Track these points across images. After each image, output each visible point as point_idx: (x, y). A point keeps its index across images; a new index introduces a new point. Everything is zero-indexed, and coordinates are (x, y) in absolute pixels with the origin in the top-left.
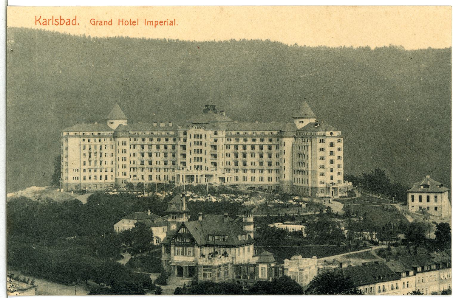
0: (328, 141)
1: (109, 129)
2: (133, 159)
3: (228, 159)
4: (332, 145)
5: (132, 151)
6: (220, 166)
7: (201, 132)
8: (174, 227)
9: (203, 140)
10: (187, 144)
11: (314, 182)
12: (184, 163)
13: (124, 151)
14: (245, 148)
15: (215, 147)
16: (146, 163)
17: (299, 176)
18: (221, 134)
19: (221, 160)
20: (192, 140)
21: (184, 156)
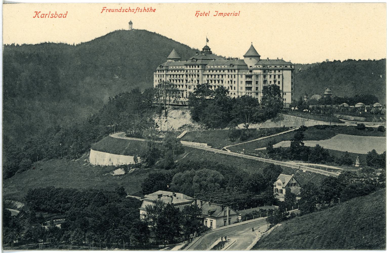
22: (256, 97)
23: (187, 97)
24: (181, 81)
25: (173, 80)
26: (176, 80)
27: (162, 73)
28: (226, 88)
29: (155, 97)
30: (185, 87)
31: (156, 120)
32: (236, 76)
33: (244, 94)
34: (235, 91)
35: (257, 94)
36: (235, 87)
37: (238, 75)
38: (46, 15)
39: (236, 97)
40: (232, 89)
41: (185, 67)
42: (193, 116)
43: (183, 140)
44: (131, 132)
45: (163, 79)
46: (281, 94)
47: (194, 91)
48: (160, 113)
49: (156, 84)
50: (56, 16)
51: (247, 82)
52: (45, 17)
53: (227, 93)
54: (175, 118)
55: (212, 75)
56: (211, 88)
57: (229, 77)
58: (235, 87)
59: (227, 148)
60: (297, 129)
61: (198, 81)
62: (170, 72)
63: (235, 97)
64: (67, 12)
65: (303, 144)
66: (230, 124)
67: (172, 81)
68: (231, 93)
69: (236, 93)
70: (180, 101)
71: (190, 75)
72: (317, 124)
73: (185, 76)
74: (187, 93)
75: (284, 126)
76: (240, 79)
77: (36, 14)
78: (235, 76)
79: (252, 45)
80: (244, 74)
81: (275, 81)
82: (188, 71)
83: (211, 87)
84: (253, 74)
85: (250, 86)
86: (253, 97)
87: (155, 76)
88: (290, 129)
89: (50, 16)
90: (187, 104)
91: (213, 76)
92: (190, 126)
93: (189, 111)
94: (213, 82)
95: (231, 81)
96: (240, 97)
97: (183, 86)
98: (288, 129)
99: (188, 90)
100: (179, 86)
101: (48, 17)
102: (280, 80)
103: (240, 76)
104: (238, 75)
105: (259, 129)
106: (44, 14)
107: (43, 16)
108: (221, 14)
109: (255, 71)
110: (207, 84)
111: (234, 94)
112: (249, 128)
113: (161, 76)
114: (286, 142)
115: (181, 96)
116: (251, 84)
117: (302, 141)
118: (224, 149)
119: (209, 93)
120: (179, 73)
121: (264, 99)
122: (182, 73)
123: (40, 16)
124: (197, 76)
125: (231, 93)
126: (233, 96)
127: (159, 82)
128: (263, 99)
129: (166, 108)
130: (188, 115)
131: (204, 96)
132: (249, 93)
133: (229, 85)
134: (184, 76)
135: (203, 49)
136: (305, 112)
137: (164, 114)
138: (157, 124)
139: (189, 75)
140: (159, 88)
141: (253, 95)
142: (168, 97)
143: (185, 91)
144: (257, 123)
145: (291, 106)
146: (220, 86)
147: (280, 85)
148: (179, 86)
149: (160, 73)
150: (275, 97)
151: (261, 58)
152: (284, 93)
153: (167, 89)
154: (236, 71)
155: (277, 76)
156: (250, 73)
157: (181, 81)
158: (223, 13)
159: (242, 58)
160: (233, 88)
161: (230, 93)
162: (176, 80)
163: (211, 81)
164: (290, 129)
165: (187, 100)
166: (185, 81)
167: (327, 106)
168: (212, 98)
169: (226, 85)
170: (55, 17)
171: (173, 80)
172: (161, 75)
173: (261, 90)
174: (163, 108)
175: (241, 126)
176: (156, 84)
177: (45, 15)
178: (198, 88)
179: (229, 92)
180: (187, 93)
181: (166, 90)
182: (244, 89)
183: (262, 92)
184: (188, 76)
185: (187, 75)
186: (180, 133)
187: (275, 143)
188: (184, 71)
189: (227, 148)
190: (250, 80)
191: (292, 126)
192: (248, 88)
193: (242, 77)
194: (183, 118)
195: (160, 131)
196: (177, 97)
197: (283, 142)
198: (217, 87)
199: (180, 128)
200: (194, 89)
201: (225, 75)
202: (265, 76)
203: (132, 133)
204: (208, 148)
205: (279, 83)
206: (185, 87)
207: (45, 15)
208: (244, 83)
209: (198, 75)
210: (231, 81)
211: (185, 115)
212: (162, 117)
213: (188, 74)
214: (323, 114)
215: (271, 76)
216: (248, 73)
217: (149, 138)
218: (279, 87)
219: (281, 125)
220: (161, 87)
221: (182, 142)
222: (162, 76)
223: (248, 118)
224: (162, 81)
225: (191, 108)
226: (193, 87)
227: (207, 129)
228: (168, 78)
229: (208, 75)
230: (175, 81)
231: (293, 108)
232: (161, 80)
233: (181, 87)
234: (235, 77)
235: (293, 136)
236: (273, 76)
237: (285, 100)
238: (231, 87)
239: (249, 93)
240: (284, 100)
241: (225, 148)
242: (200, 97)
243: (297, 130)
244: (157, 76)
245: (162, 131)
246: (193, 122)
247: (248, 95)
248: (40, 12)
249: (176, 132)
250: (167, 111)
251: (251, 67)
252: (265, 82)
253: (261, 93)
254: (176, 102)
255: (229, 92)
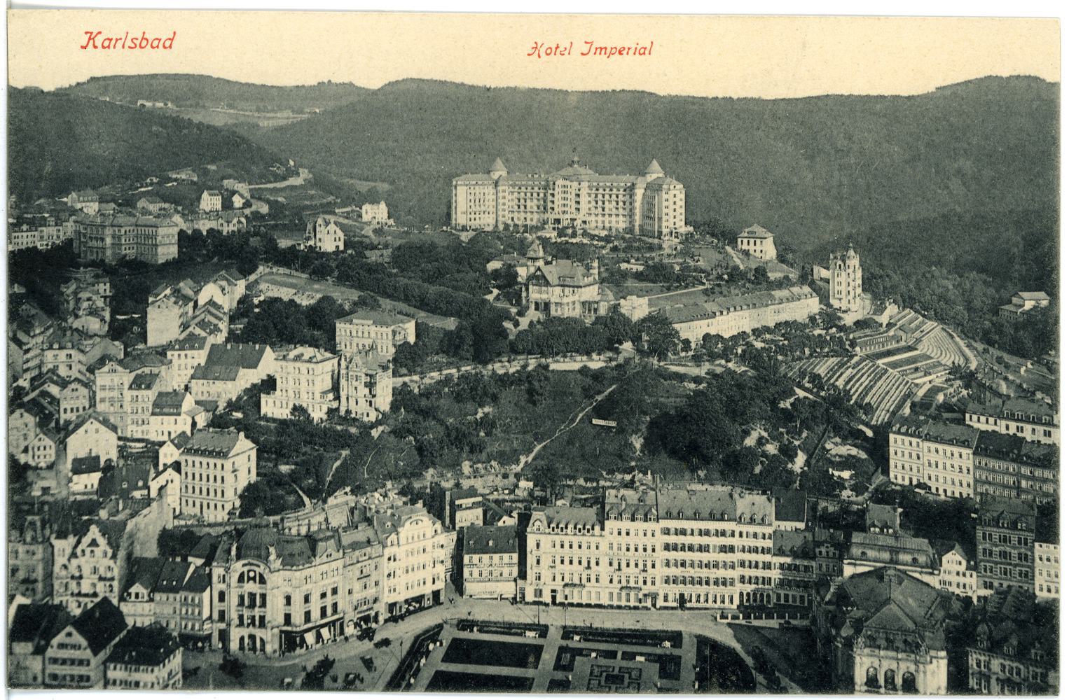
0: (672, 193)
1: (491, 179)
2: (510, 204)
3: (590, 206)
4: (675, 196)
5: (510, 197)
6: (583, 212)
7: (567, 183)
8: (532, 270)
9: (569, 189)
10: (556, 193)
11: (660, 227)
12: (553, 209)
13: (504, 198)
14: (603, 196)
15: (578, 195)
16: (522, 207)
17: (648, 221)
18: (585, 185)
19: (584, 206)
20: (560, 190)
21: (553, 202)
38: (117, 40)
50: (143, 45)
52: (114, 47)
64: (175, 33)
77: (90, 39)
89: (129, 43)
101: (123, 47)
106: (110, 40)
107: (109, 43)
108: (602, 49)
123: (98, 43)
158: (606, 48)
170: (141, 47)
177: (113, 42)
207: (113, 42)
248: (100, 33)
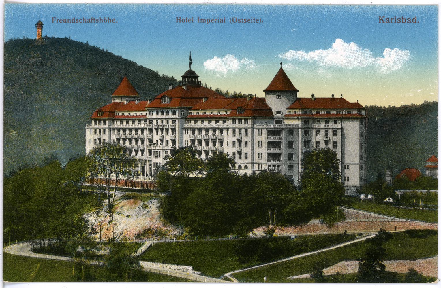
22: (288, 174)
23: (151, 173)
24: (140, 142)
25: (124, 140)
26: (130, 140)
27: (102, 126)
28: (228, 155)
29: (89, 174)
30: (148, 154)
31: (92, 219)
32: (250, 131)
33: (264, 167)
34: (246, 161)
35: (291, 167)
36: (246, 154)
37: (253, 129)
39: (249, 173)
40: (240, 157)
41: (148, 113)
42: (164, 212)
43: (144, 260)
44: (42, 242)
45: (105, 137)
46: (339, 168)
47: (165, 162)
48: (99, 205)
49: (89, 147)
51: (271, 144)
53: (230, 165)
54: (128, 216)
55: (200, 131)
56: (200, 156)
57: (234, 134)
58: (246, 154)
59: (231, 275)
60: (370, 237)
61: (174, 142)
62: (118, 124)
63: (246, 173)
65: (384, 267)
66: (237, 227)
67: (122, 142)
68: (240, 166)
69: (249, 166)
70: (138, 182)
71: (157, 130)
72: (411, 228)
73: (146, 132)
74: (151, 165)
75: (346, 231)
76: (258, 138)
78: (246, 131)
79: (281, 69)
80: (265, 126)
81: (327, 142)
82: (154, 122)
83: (200, 153)
84: (283, 127)
85: (276, 151)
86: (283, 173)
87: (87, 131)
88: (357, 237)
90: (152, 189)
91: (203, 132)
92: (158, 233)
93: (155, 201)
94: (203, 143)
95: (240, 142)
96: (257, 173)
97: (143, 151)
98: (353, 237)
99: (154, 160)
100: (137, 152)
102: (338, 139)
103: (256, 131)
104: (253, 129)
105: (296, 237)
109: (288, 122)
110: (191, 147)
111: (246, 167)
112: (274, 235)
113: (100, 132)
114: (349, 262)
115: (139, 173)
116: (280, 147)
117: (380, 262)
118: (226, 276)
119: (196, 165)
120: (136, 125)
121: (305, 176)
122: (142, 125)
124: (170, 132)
125: (240, 166)
126: (242, 172)
127: (95, 143)
128: (302, 177)
129: (111, 196)
130: (154, 207)
131: (186, 173)
132: (274, 166)
133: (235, 150)
134: (145, 131)
135: (184, 77)
136: (387, 203)
137: (105, 208)
138: (94, 227)
139: (155, 129)
140: (96, 156)
141: (284, 170)
142: (114, 174)
143: (147, 161)
144: (291, 226)
145: (359, 191)
146: (218, 153)
147: (338, 150)
148: (137, 152)
149: (98, 126)
150: (327, 173)
151: (299, 95)
152: (345, 166)
153: (111, 157)
154: (250, 122)
155: (331, 133)
156: (277, 125)
157: (140, 142)
159: (261, 95)
160: (243, 155)
161: (237, 165)
162: (130, 140)
163: (200, 142)
164: (357, 237)
165: (152, 179)
166: (147, 142)
167: (431, 191)
168: (200, 176)
169: (229, 150)
171: (124, 140)
172: (100, 130)
173: (300, 159)
174: (105, 196)
175: (259, 232)
176: (89, 147)
178: (173, 156)
179: (236, 163)
180: (151, 165)
181: (110, 159)
182: (265, 156)
183: (302, 164)
184: (154, 132)
185: (151, 130)
186: (140, 245)
187: (327, 265)
188: (146, 121)
189: (231, 275)
190: (277, 139)
191: (363, 231)
192: (272, 156)
193: (260, 133)
194: (144, 217)
195: (98, 240)
196: (131, 175)
197: (344, 262)
198: (211, 154)
199: (138, 235)
200: (166, 157)
201: (227, 129)
202: (306, 132)
203: (44, 244)
204: (194, 274)
205: (335, 145)
206: (147, 153)
208: (265, 146)
209: (174, 130)
210: (240, 142)
211: (148, 209)
212: (103, 213)
213: (154, 127)
214: (423, 208)
215: (318, 131)
216: (273, 126)
217: (79, 255)
218: (335, 154)
219: (340, 228)
220: (100, 153)
221: (142, 263)
222: (102, 131)
223: (273, 214)
224: (102, 141)
225: (160, 195)
226: (163, 155)
227: (192, 237)
228: (114, 137)
229: (193, 131)
230: (127, 142)
231: (362, 196)
232: (100, 139)
233: (140, 153)
234: (246, 134)
235: (363, 251)
236: (322, 132)
237: (348, 180)
238: (240, 153)
239: (274, 166)
240: (345, 180)
241: (227, 275)
242: (177, 174)
243: (372, 240)
244: (93, 130)
245: (101, 242)
246: (165, 224)
247: (273, 170)
249: (130, 244)
250: (113, 202)
251: (278, 112)
252: (307, 143)
253: (300, 166)
254: (130, 184)
255: (236, 163)
